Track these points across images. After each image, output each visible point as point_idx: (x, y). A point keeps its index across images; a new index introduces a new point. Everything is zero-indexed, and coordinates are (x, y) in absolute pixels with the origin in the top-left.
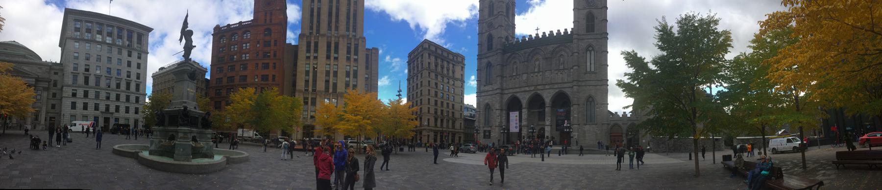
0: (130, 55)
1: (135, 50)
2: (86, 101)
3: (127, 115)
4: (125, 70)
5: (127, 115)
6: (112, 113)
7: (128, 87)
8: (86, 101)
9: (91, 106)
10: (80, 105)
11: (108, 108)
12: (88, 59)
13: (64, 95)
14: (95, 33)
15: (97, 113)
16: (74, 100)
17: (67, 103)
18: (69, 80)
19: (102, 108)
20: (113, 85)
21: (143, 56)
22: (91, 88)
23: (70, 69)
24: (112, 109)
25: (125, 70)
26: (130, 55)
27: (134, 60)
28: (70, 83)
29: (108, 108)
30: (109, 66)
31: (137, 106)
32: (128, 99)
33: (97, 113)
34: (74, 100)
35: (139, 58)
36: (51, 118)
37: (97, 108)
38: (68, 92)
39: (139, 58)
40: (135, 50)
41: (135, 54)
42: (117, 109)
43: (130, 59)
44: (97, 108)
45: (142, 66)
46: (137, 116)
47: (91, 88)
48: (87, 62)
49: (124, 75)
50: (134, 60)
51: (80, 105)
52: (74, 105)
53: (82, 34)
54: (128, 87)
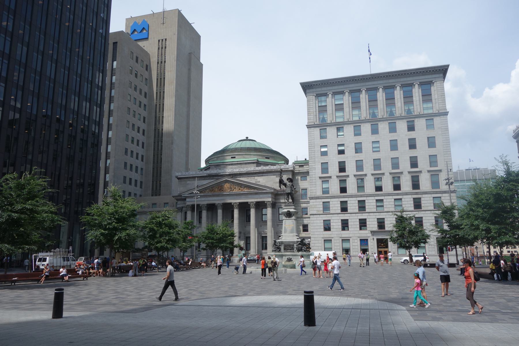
0: (411, 128)
2: (345, 217)
4: (404, 155)
8: (345, 217)
15: (365, 234)
16: (326, 217)
19: (372, 225)
22: (352, 196)
23: (316, 171)
26: (411, 128)
27: (421, 133)
28: (319, 193)
30: (376, 156)
33: (365, 234)
35: (430, 126)
37: (363, 224)
41: (420, 124)
44: (363, 224)
45: (438, 142)
47: (352, 196)
49: (387, 167)
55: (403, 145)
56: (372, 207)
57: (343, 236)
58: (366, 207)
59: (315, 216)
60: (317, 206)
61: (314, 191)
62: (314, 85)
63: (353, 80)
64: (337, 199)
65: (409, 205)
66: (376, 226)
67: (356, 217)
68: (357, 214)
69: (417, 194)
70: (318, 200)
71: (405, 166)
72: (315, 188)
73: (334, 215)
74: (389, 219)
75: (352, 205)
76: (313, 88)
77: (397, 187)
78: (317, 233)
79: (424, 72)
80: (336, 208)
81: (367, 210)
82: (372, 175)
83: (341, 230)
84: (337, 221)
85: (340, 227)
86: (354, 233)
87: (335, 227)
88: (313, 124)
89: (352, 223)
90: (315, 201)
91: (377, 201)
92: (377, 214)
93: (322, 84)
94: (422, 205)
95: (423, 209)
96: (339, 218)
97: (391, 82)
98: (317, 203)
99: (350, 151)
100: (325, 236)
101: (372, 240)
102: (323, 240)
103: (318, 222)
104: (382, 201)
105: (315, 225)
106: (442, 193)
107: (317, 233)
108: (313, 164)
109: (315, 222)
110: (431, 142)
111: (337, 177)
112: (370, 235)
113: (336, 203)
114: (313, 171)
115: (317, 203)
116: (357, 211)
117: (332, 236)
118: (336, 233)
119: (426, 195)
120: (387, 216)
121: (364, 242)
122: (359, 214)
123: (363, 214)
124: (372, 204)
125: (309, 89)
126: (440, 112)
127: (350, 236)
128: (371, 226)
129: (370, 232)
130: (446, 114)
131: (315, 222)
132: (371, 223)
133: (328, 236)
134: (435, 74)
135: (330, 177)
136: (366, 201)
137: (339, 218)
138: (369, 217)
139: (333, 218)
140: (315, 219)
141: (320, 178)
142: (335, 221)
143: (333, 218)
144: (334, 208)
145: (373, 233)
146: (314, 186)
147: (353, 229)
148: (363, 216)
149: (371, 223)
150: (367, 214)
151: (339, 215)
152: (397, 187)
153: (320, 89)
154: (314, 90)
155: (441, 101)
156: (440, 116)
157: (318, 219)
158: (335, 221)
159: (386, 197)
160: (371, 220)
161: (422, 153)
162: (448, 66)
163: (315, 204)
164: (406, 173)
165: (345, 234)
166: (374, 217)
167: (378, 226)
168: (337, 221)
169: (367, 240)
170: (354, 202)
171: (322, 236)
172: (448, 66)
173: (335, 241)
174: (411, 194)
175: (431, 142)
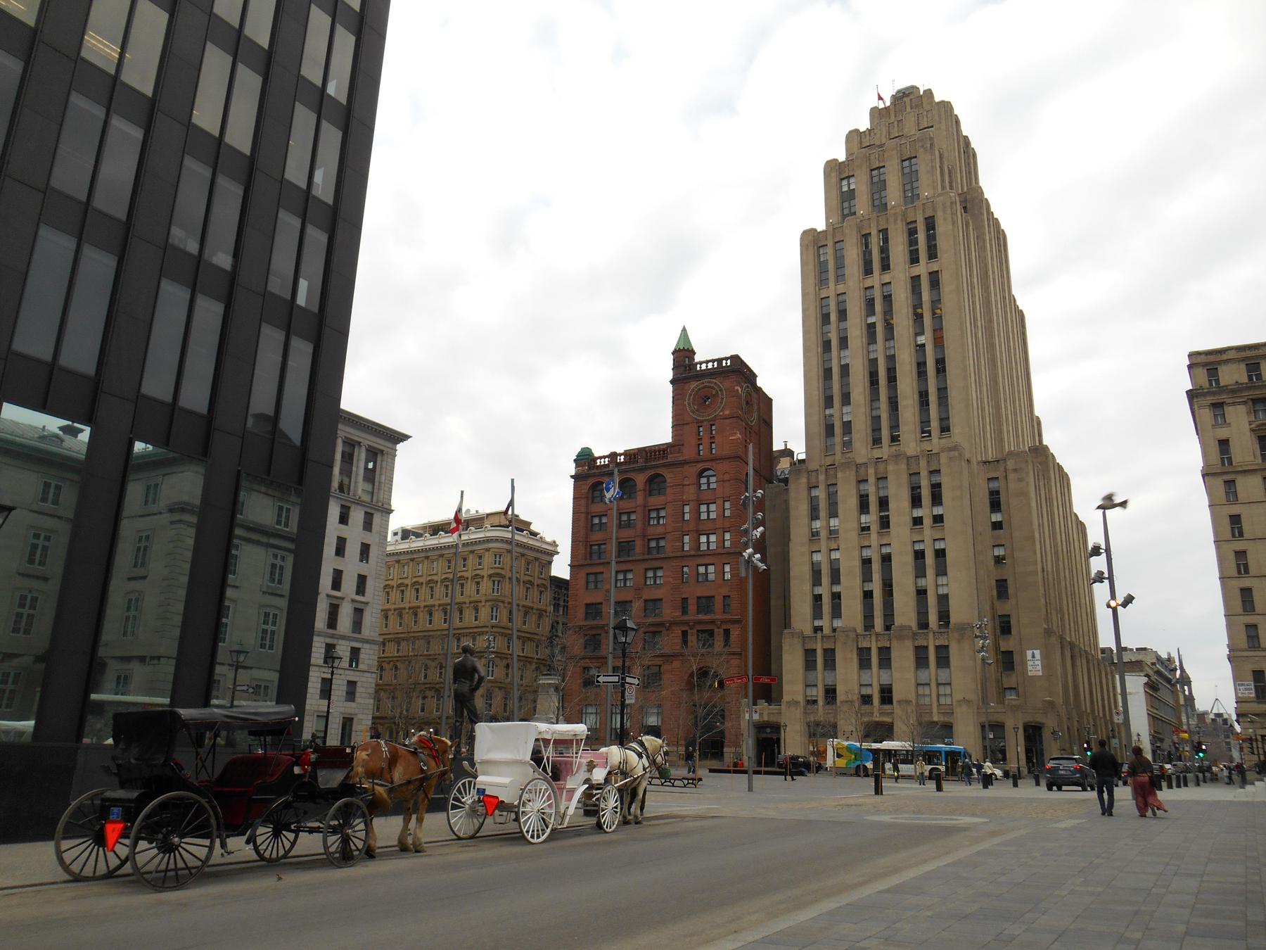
0: (344, 519)
1: (359, 503)
21: (377, 519)
35: (368, 525)
39: (368, 525)
40: (359, 503)
41: (357, 516)
43: (344, 531)
46: (350, 708)
69: (332, 636)
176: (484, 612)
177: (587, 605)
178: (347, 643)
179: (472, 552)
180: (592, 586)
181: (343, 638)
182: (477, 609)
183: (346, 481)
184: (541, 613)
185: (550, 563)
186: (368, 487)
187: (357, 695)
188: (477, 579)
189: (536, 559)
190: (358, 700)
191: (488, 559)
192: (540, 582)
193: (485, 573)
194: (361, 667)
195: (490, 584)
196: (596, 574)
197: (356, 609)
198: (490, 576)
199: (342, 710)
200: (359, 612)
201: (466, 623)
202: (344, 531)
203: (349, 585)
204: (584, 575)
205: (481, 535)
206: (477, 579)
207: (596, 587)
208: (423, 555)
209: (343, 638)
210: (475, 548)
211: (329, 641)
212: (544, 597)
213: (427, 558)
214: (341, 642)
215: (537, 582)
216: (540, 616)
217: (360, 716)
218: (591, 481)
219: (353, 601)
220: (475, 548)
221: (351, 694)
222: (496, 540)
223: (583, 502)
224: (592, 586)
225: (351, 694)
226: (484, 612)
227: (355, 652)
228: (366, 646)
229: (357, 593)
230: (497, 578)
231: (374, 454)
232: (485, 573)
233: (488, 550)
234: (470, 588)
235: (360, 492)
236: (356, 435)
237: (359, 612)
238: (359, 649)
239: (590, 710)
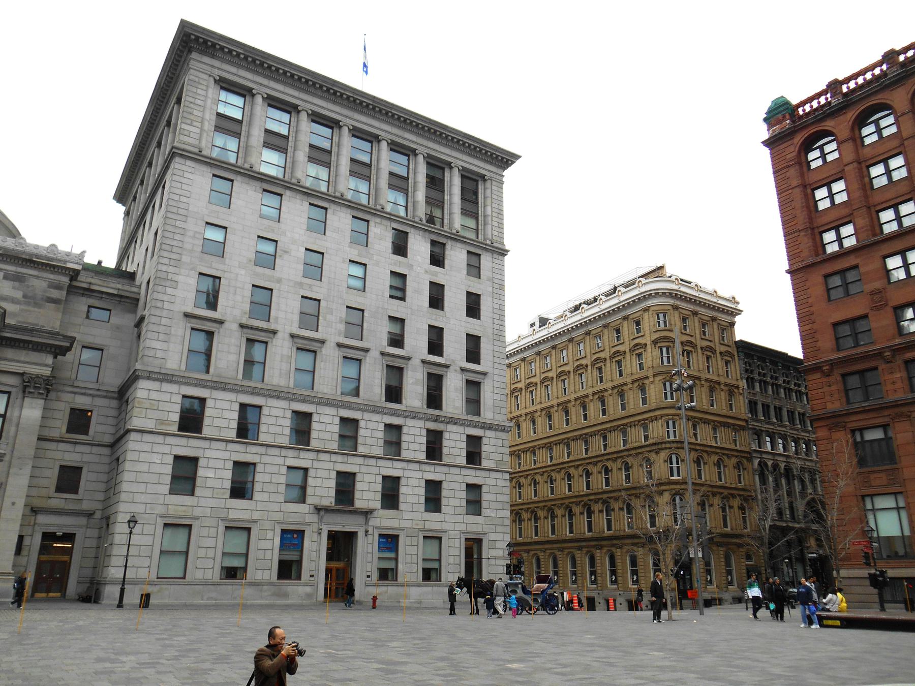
0: (437, 260)
1: (457, 238)
3: (434, 521)
4: (418, 318)
5: (434, 521)
6: (366, 513)
7: (434, 399)
9: (271, 473)
10: (215, 473)
11: (346, 485)
12: (268, 261)
13: (137, 421)
14: (302, 155)
16: (186, 446)
17: (147, 463)
18: (168, 346)
19: (323, 489)
20: (374, 382)
21: (486, 261)
24: (368, 493)
25: (418, 318)
26: (437, 260)
27: (455, 278)
29: (346, 485)
31: (473, 476)
32: (434, 450)
34: (186, 446)
35: (474, 269)
36: (48, 537)
38: (156, 404)
39: (474, 269)
40: (457, 238)
41: (456, 256)
42: (391, 494)
43: (439, 275)
45: (486, 306)
46: (475, 525)
48: (264, 277)
50: (455, 278)
51: (215, 473)
52: (185, 473)
53: (245, 150)
54: (434, 399)
55: (418, 293)
56: (327, 436)
57: (233, 515)
58: (314, 434)
59: (148, 437)
60: (162, 406)
61: (159, 354)
62: (222, 48)
63: (328, 90)
64: (232, 396)
65: (417, 447)
66: (333, 493)
67: (280, 461)
68: (284, 452)
69: (436, 419)
70: (166, 387)
71: (416, 342)
72: (164, 346)
73: (215, 445)
74: (367, 478)
75: (272, 420)
76: (213, 56)
77: (394, 394)
78: (143, 498)
79: (475, 147)
80: (224, 423)
81: (314, 444)
82: (339, 345)
83: (228, 495)
84: (220, 464)
85: (228, 485)
86: (269, 507)
87: (210, 483)
88: (196, 150)
89: (267, 478)
90: (155, 385)
91: (343, 420)
92: (339, 458)
93: (246, 58)
94: (445, 451)
95: (446, 460)
96: (226, 455)
97: (409, 138)
98: (166, 397)
99: (290, 268)
100: (172, 511)
101: (316, 535)
102: (160, 522)
103: (156, 459)
104: (356, 422)
105: (144, 467)
106: (485, 428)
107: (143, 498)
108: (171, 269)
109: (143, 456)
110: (473, 307)
111: (242, 326)
112: (314, 518)
113: (226, 405)
114: (169, 291)
115: (166, 397)
116: (285, 440)
117: (197, 512)
118: (213, 503)
119: (454, 428)
120: (364, 469)
121: (292, 538)
122: (290, 453)
123: (303, 454)
124: (330, 428)
125: (202, 53)
126: (495, 244)
127: (256, 516)
128: (319, 492)
129: (312, 507)
130: (503, 253)
131: (143, 456)
132: (318, 482)
133: (180, 511)
134: (491, 163)
135: (221, 322)
136: (315, 418)
137: (226, 455)
138: (316, 464)
139: (209, 453)
140: (146, 447)
141: (187, 315)
142: (212, 463)
143: (209, 453)
144: (217, 422)
145: (318, 509)
146: (162, 337)
147: (265, 497)
148: (304, 460)
149: (318, 482)
150: (312, 455)
151: (231, 446)
152: (394, 394)
153: (233, 70)
154: (217, 63)
155: (496, 224)
156: (493, 252)
157: (157, 448)
158: (212, 463)
159: (367, 416)
160: (320, 473)
161: (456, 324)
162: (518, 157)
163: (154, 395)
164: (416, 362)
165: (240, 510)
166: (330, 466)
167: (338, 492)
168: (220, 464)
169: (301, 533)
170: (280, 413)
171: (160, 510)
172: (518, 157)
173: (204, 532)
174: (426, 419)
175: (473, 307)
176: (655, 392)
177: (835, 325)
178: (460, 429)
179: (625, 318)
180: (837, 294)
181: (454, 421)
182: (643, 389)
183: (437, 213)
184: (732, 390)
185: (732, 324)
186: (471, 223)
187: (484, 504)
188: (638, 350)
189: (714, 319)
190: (485, 512)
191: (649, 323)
192: (723, 349)
193: (647, 340)
194: (485, 463)
195: (657, 352)
196: (842, 272)
197: (469, 383)
198: (655, 342)
199: (463, 527)
200: (473, 386)
201: (632, 408)
202: (439, 275)
203: (454, 349)
204: (820, 279)
205: (636, 292)
206: (638, 350)
207: (847, 294)
208: (565, 339)
209: (454, 421)
210: (629, 312)
211: (432, 426)
212: (732, 367)
213: (571, 340)
214: (450, 427)
215: (719, 348)
216: (731, 394)
217: (493, 536)
218: (799, 139)
219: (463, 370)
220: (629, 312)
221: (474, 504)
222: (656, 294)
223: (793, 172)
224: (837, 294)
225: (474, 504)
226: (655, 392)
227: (474, 442)
228: (489, 433)
229: (469, 360)
230: (663, 342)
231: (472, 185)
232: (647, 340)
233: (646, 310)
234: (630, 365)
235: (457, 225)
236: (444, 152)
237: (473, 386)
238: (479, 439)
239: (881, 503)
